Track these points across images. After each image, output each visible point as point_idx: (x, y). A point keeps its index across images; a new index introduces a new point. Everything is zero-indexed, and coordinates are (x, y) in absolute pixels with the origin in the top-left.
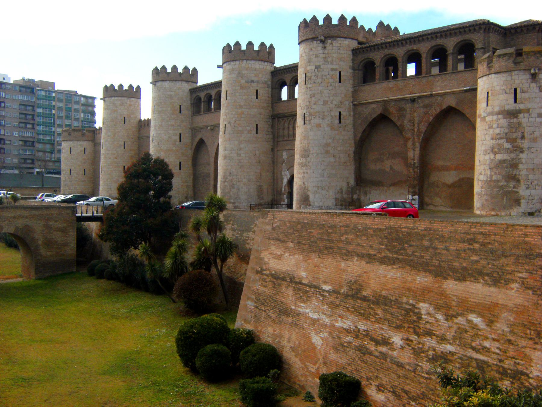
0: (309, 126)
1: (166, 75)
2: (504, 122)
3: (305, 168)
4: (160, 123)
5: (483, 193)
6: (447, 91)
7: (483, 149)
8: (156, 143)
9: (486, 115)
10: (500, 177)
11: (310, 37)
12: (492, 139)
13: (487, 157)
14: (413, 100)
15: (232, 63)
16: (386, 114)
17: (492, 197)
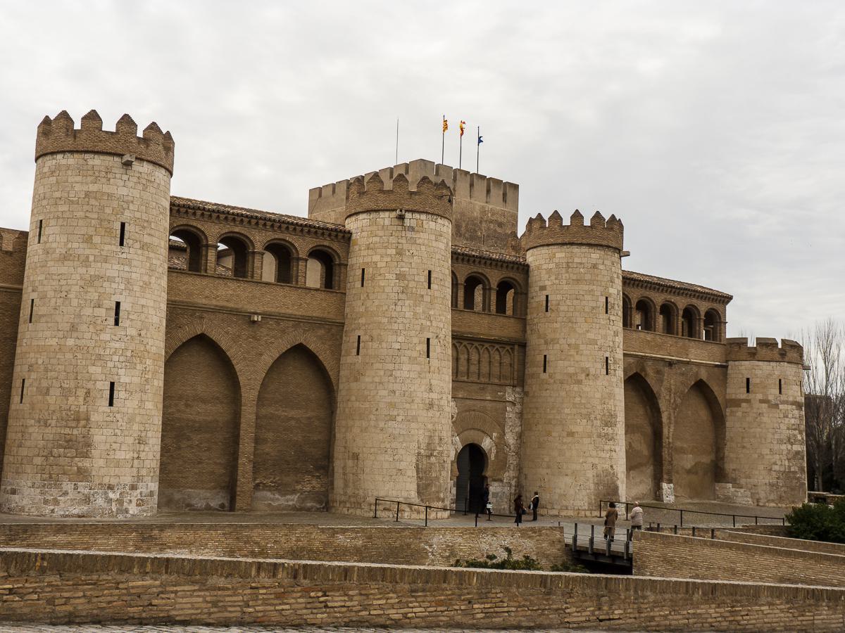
0: (614, 379)
1: (163, 153)
2: (796, 412)
3: (611, 442)
4: (146, 278)
5: (781, 484)
6: (717, 363)
7: (776, 436)
8: (134, 332)
9: (779, 402)
10: (797, 469)
11: (614, 245)
12: (788, 429)
13: (784, 447)
14: (670, 364)
15: (439, 220)
16: (643, 374)
17: (792, 489)
